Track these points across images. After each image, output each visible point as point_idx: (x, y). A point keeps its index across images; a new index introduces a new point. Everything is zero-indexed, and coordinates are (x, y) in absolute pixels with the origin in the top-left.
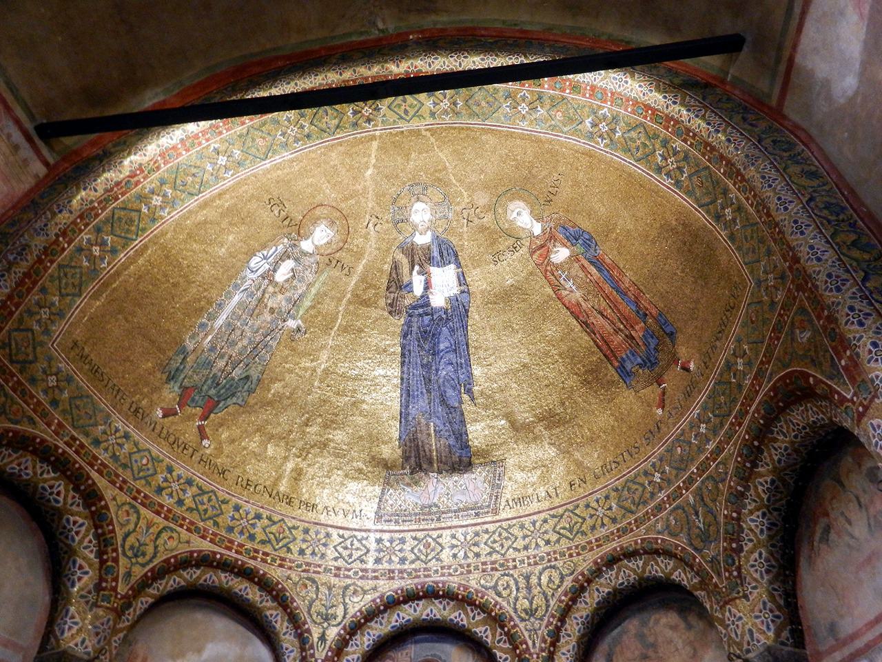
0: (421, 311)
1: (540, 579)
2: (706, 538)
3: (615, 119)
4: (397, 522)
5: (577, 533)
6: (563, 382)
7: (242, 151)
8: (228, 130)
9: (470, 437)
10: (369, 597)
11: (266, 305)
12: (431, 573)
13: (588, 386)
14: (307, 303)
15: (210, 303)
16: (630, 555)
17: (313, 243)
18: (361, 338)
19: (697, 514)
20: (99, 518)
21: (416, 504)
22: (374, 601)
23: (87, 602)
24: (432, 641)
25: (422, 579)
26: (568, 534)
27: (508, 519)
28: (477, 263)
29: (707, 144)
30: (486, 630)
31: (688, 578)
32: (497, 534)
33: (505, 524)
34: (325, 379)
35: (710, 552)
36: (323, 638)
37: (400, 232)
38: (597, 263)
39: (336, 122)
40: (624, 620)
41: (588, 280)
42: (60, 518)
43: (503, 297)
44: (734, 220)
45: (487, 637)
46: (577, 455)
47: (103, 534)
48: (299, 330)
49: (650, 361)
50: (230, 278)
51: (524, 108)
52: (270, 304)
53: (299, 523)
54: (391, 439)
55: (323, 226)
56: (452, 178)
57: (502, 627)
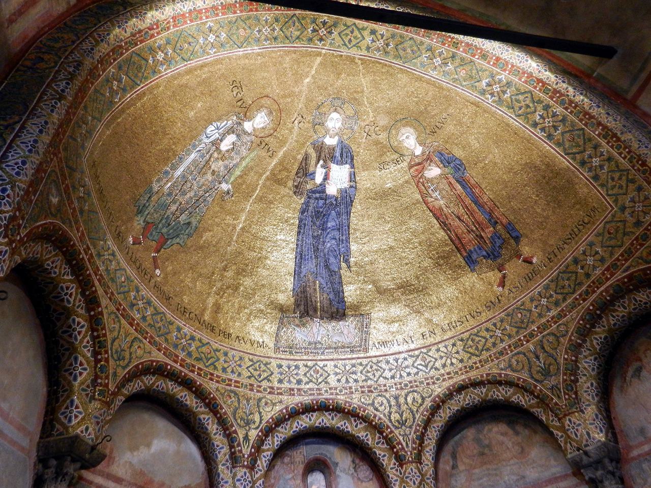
0: (318, 195)
1: (406, 399)
2: (546, 373)
3: (509, 84)
4: (291, 353)
5: (432, 368)
6: (420, 263)
7: (227, 35)
8: (223, 14)
9: (346, 294)
10: (278, 408)
11: (210, 167)
12: (323, 392)
13: (440, 267)
14: (238, 173)
15: (175, 155)
16: (475, 384)
17: (253, 125)
18: (270, 208)
19: (538, 357)
20: (95, 322)
21: (305, 340)
22: (281, 411)
23: (87, 395)
24: (318, 443)
25: (316, 397)
26: (424, 369)
27: (375, 357)
28: (366, 167)
29: (586, 113)
30: (367, 435)
31: (525, 400)
32: (369, 366)
33: (374, 360)
34: (241, 235)
35: (553, 381)
36: (246, 438)
37: (315, 132)
38: (463, 182)
39: (298, 33)
40: (463, 429)
42: (68, 318)
43: (382, 196)
44: (601, 167)
45: (368, 440)
46: (427, 315)
47: (98, 337)
48: (228, 193)
49: (494, 255)
51: (438, 61)
53: (220, 347)
54: (286, 289)
55: (263, 113)
56: (365, 99)
57: (381, 433)
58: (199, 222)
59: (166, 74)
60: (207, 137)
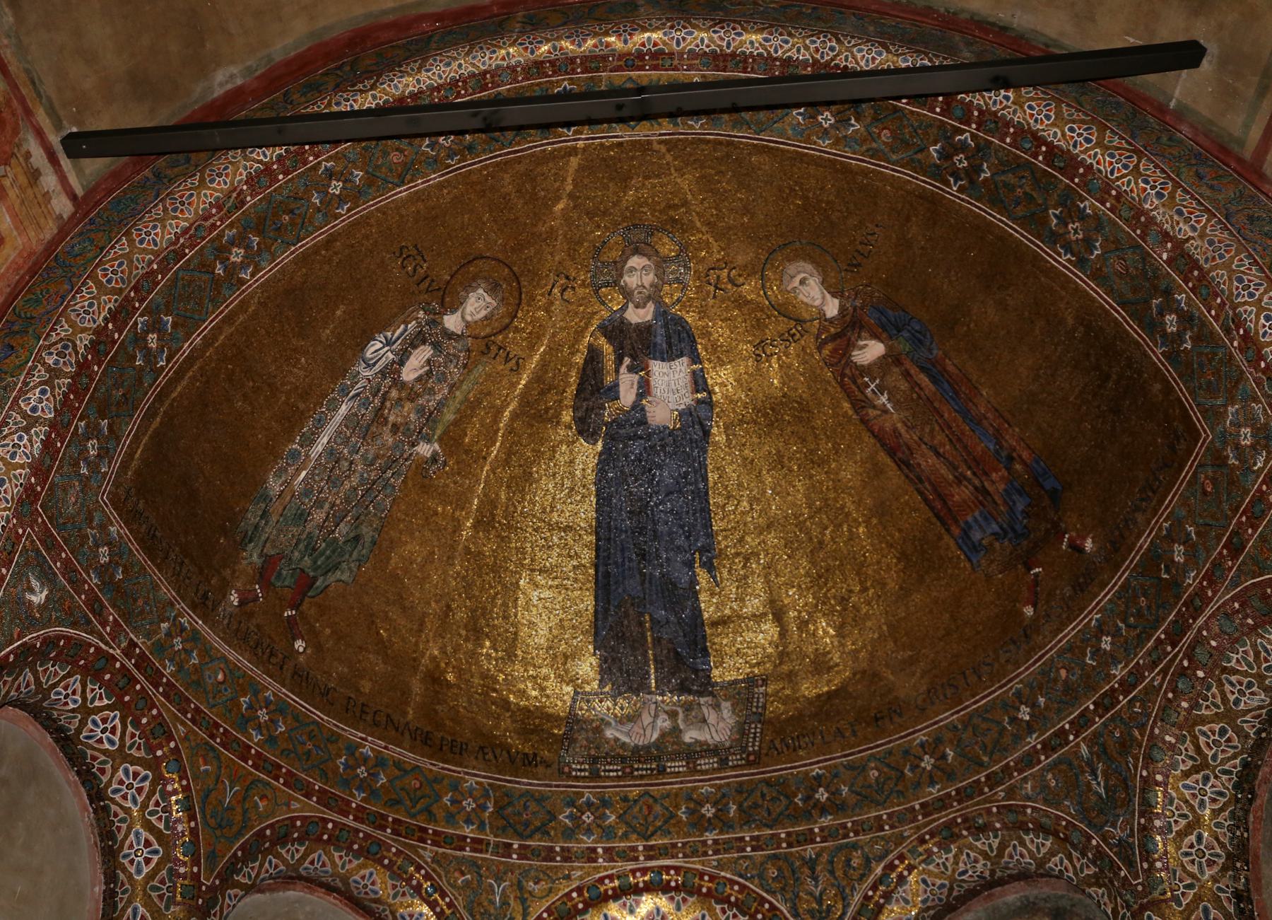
11: (386, 419)
14: (449, 416)
17: (463, 317)
41: (915, 396)
48: (434, 459)
50: (334, 379)
52: (392, 418)
55: (481, 291)
56: (696, 219)
58: (380, 531)
59: (257, 281)
60: (369, 365)
